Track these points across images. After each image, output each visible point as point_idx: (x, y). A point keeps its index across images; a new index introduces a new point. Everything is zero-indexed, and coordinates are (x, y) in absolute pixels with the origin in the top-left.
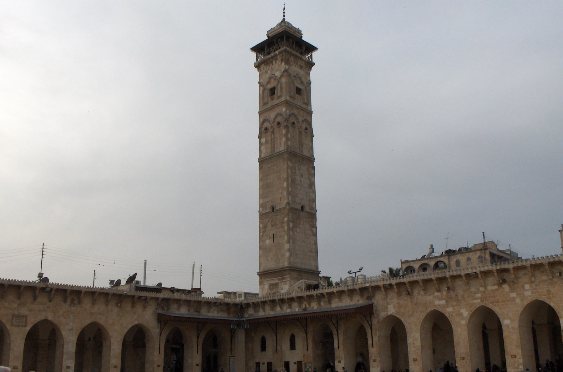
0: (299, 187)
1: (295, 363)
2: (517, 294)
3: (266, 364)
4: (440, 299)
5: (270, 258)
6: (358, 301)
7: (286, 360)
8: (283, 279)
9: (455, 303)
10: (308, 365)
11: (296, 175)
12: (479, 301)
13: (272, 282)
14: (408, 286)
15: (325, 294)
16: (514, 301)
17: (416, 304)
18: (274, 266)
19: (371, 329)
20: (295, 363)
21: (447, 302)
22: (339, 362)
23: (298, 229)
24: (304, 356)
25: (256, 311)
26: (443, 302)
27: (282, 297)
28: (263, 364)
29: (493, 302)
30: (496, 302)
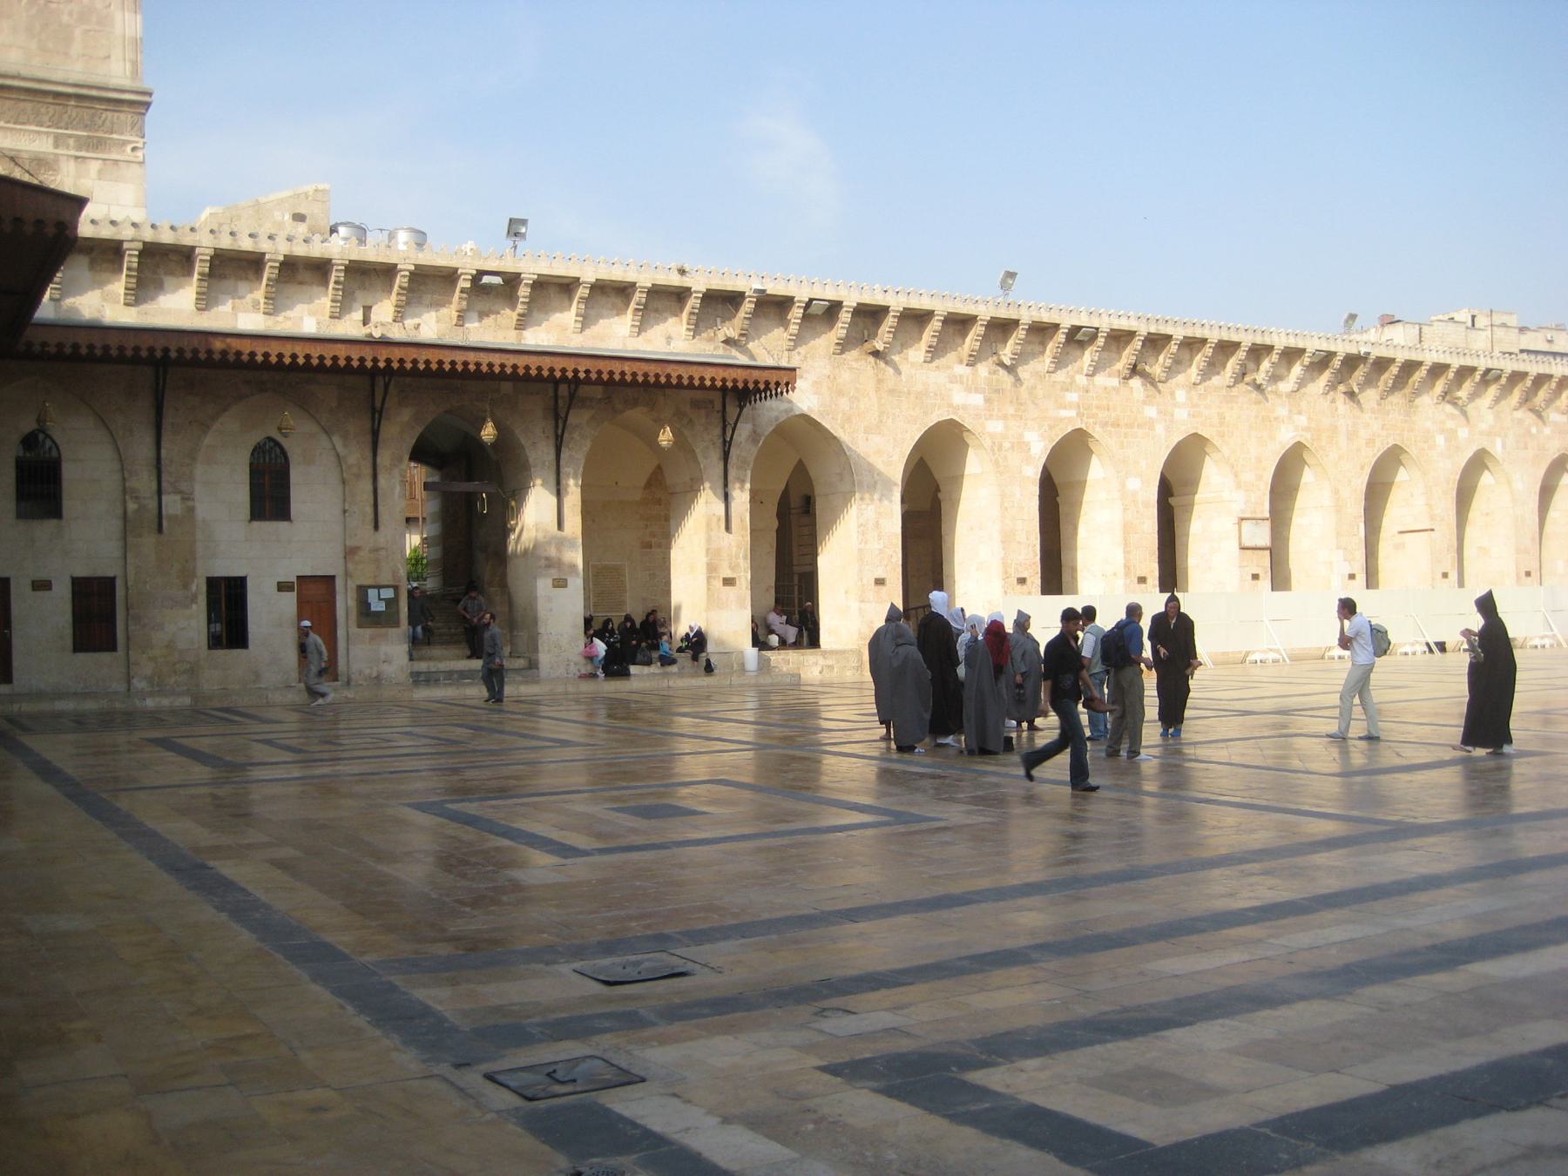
1: (283, 587)
2: (1159, 412)
3: (62, 592)
4: (969, 390)
6: (669, 339)
8: (97, 144)
9: (1011, 410)
10: (372, 593)
12: (1072, 413)
16: (1152, 428)
17: (892, 392)
19: (726, 457)
20: (283, 587)
21: (987, 400)
22: (560, 583)
25: (142, 290)
26: (977, 400)
28: (42, 585)
29: (1106, 424)
30: (1113, 425)
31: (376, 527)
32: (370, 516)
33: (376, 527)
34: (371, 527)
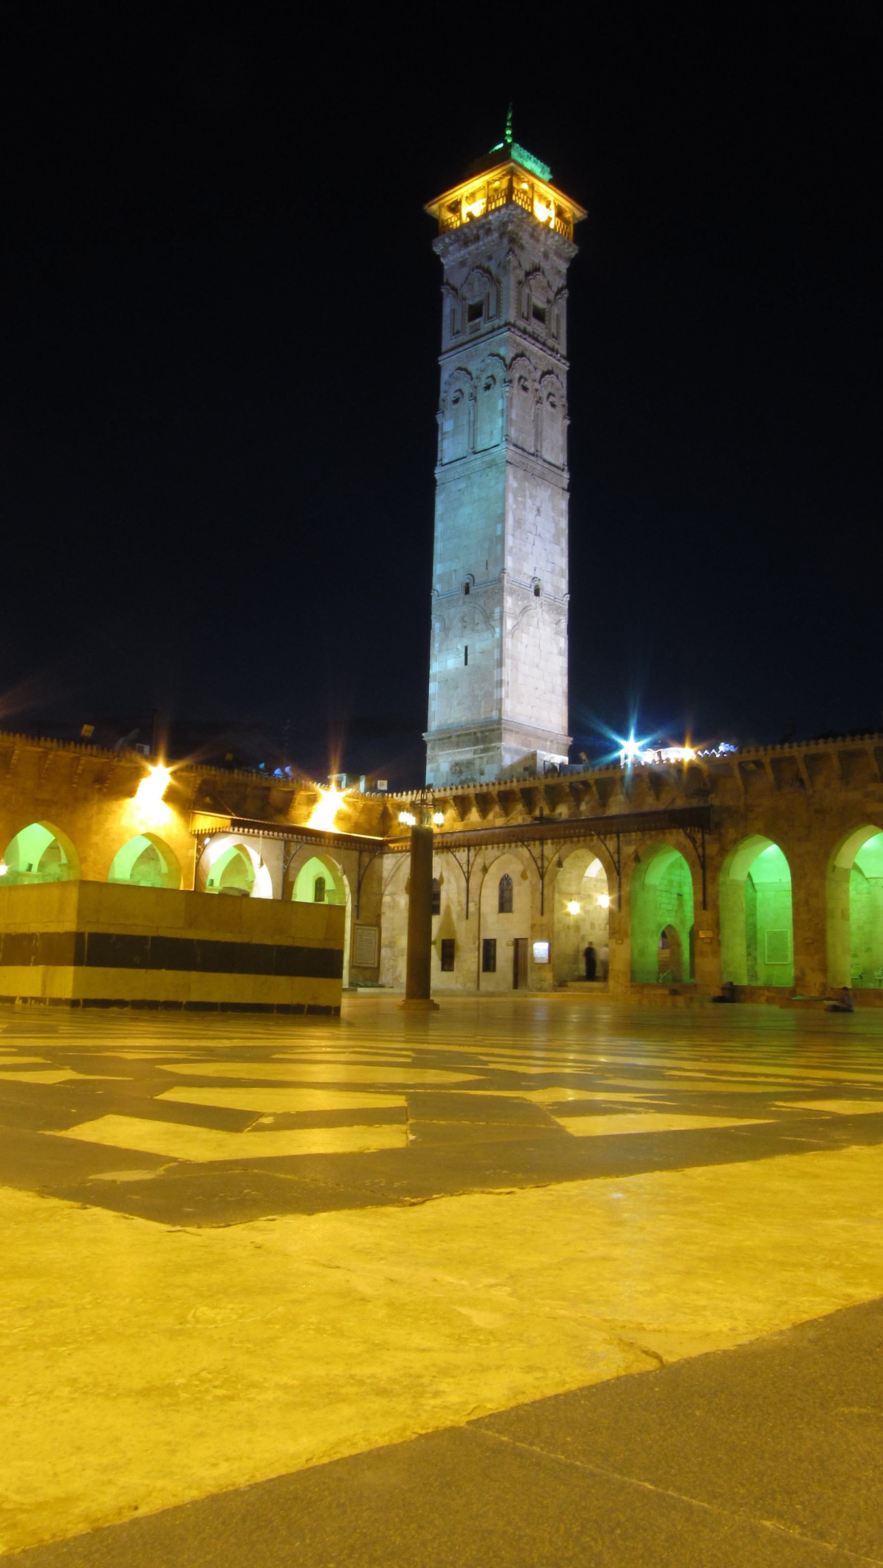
0: (531, 537)
5: (455, 703)
7: (490, 936)
11: (524, 508)
13: (458, 758)
14: (802, 766)
15: (592, 782)
18: (464, 719)
23: (524, 636)
24: (533, 926)
27: (485, 789)
31: (542, 914)
32: (540, 910)
33: (542, 914)
34: (539, 914)
